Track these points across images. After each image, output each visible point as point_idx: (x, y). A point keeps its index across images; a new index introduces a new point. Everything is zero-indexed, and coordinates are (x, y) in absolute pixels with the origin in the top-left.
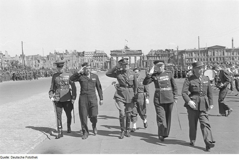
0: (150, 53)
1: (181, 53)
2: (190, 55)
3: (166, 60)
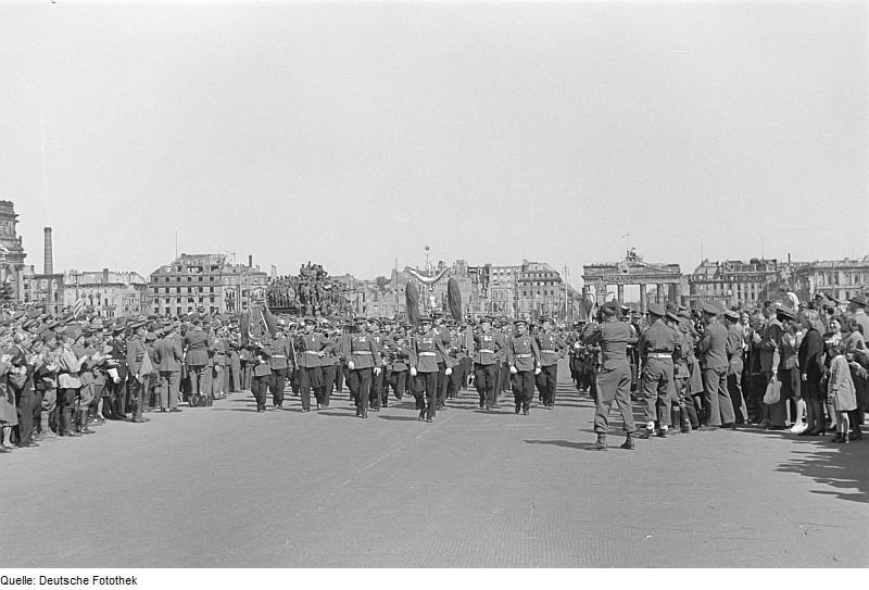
0: (700, 272)
1: (805, 271)
2: (830, 279)
3: (753, 295)
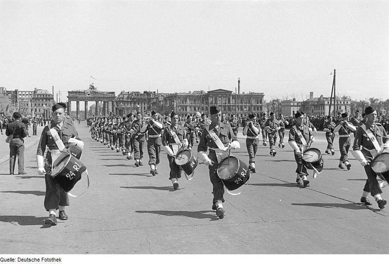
3: (145, 108)
